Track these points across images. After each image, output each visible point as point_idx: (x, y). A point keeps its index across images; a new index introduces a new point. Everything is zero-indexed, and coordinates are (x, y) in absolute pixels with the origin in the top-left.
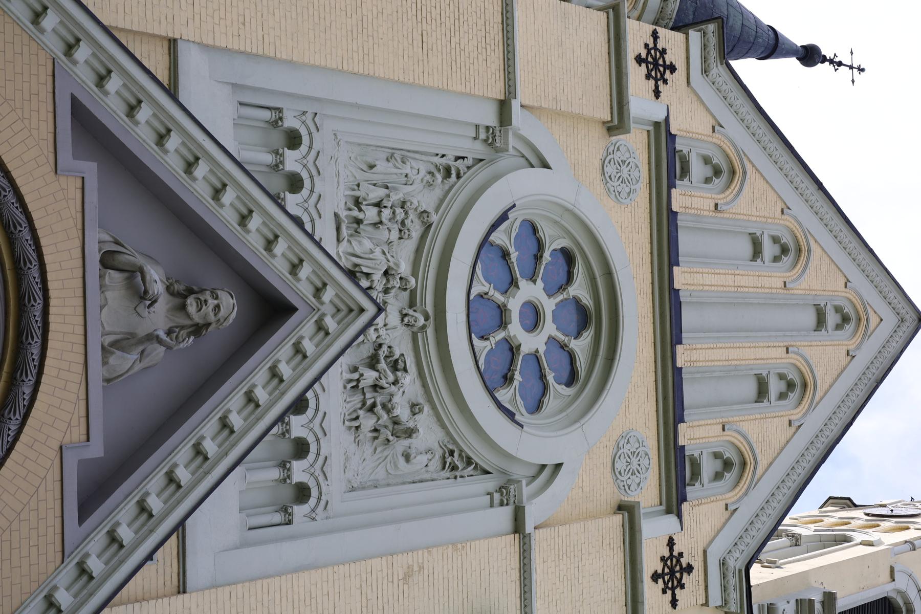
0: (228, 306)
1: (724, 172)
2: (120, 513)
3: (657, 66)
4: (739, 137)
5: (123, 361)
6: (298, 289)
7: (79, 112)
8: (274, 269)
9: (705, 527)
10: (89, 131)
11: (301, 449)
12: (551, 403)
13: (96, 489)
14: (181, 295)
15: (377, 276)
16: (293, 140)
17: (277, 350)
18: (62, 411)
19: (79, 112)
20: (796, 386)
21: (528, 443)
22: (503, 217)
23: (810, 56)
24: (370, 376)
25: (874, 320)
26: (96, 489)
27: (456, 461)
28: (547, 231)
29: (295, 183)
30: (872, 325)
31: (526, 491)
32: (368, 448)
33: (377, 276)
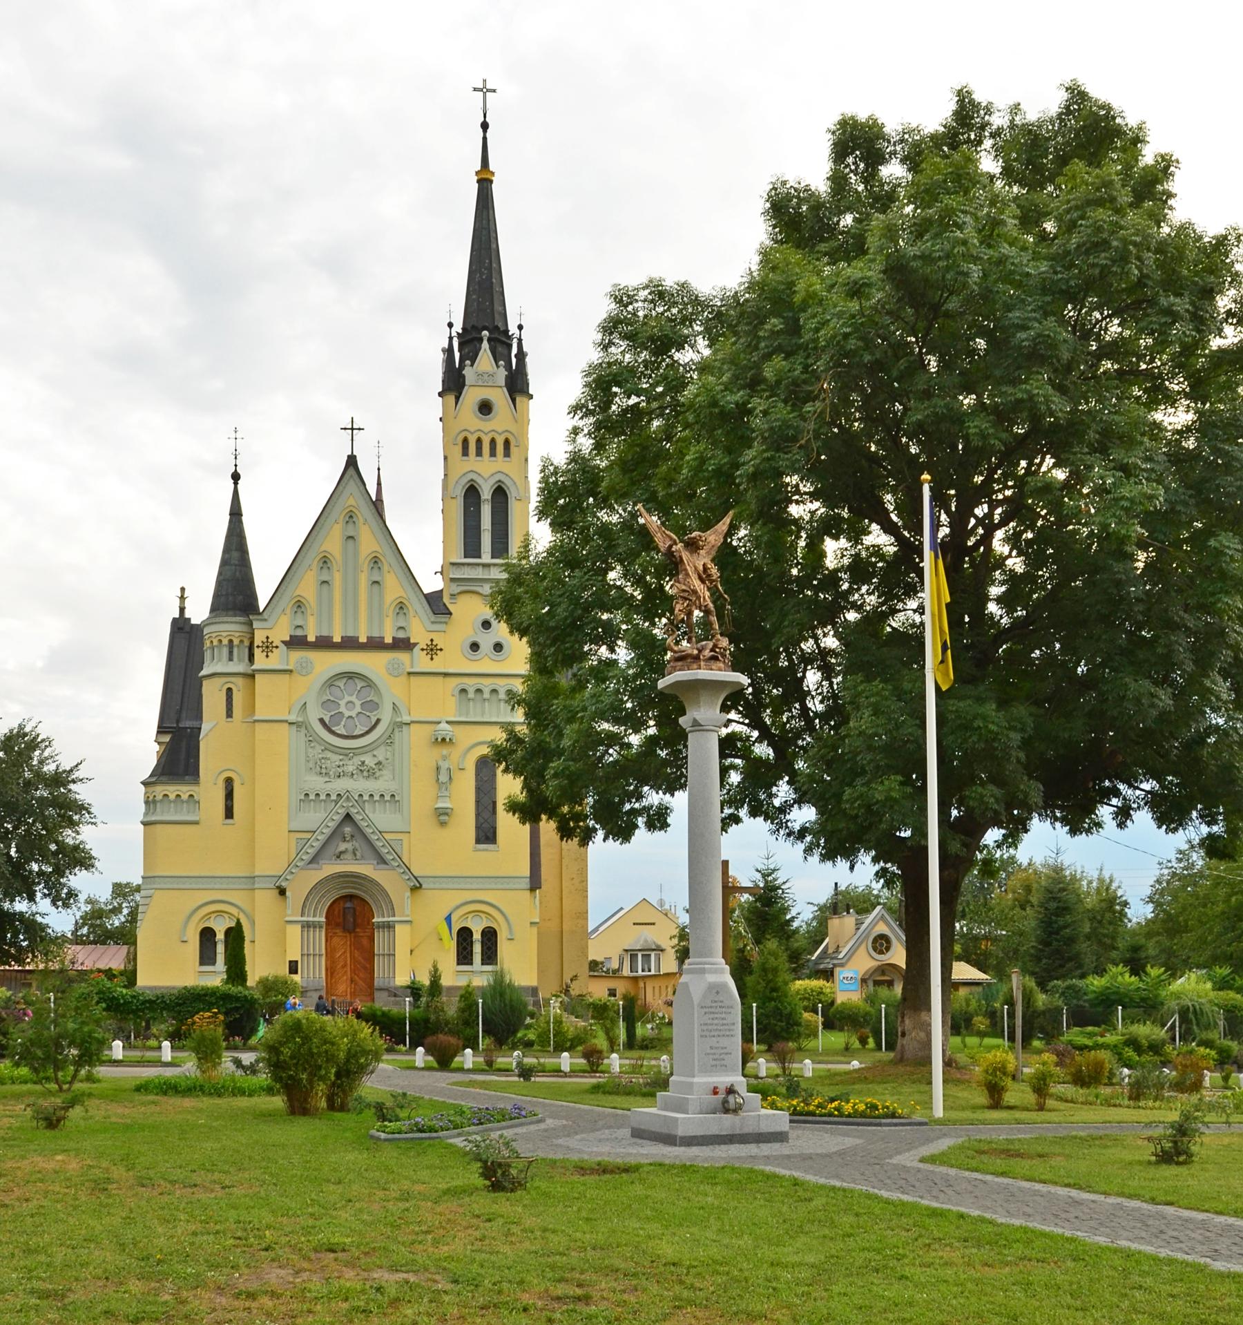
0: (348, 830)
1: (299, 605)
2: (390, 857)
3: (268, 647)
4: (286, 602)
5: (358, 854)
6: (342, 811)
7: (310, 862)
8: (338, 818)
9: (419, 631)
10: (314, 860)
11: (382, 796)
12: (375, 699)
13: (382, 861)
14: (344, 840)
15: (340, 770)
16: (307, 795)
17: (357, 818)
18: (366, 869)
19: (310, 862)
20: (376, 561)
21: (386, 716)
22: (322, 721)
23: (236, 477)
24: (365, 774)
25: (351, 502)
26: (382, 861)
27: (388, 741)
28: (325, 698)
29: (317, 795)
30: (353, 503)
31: (399, 720)
32: (384, 772)
33: (340, 770)
